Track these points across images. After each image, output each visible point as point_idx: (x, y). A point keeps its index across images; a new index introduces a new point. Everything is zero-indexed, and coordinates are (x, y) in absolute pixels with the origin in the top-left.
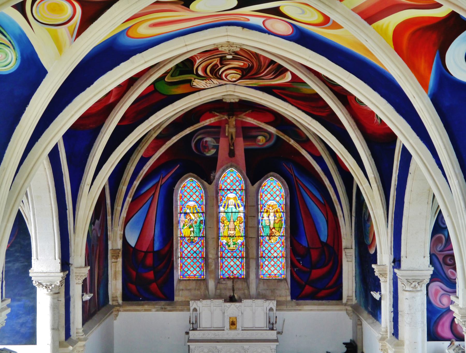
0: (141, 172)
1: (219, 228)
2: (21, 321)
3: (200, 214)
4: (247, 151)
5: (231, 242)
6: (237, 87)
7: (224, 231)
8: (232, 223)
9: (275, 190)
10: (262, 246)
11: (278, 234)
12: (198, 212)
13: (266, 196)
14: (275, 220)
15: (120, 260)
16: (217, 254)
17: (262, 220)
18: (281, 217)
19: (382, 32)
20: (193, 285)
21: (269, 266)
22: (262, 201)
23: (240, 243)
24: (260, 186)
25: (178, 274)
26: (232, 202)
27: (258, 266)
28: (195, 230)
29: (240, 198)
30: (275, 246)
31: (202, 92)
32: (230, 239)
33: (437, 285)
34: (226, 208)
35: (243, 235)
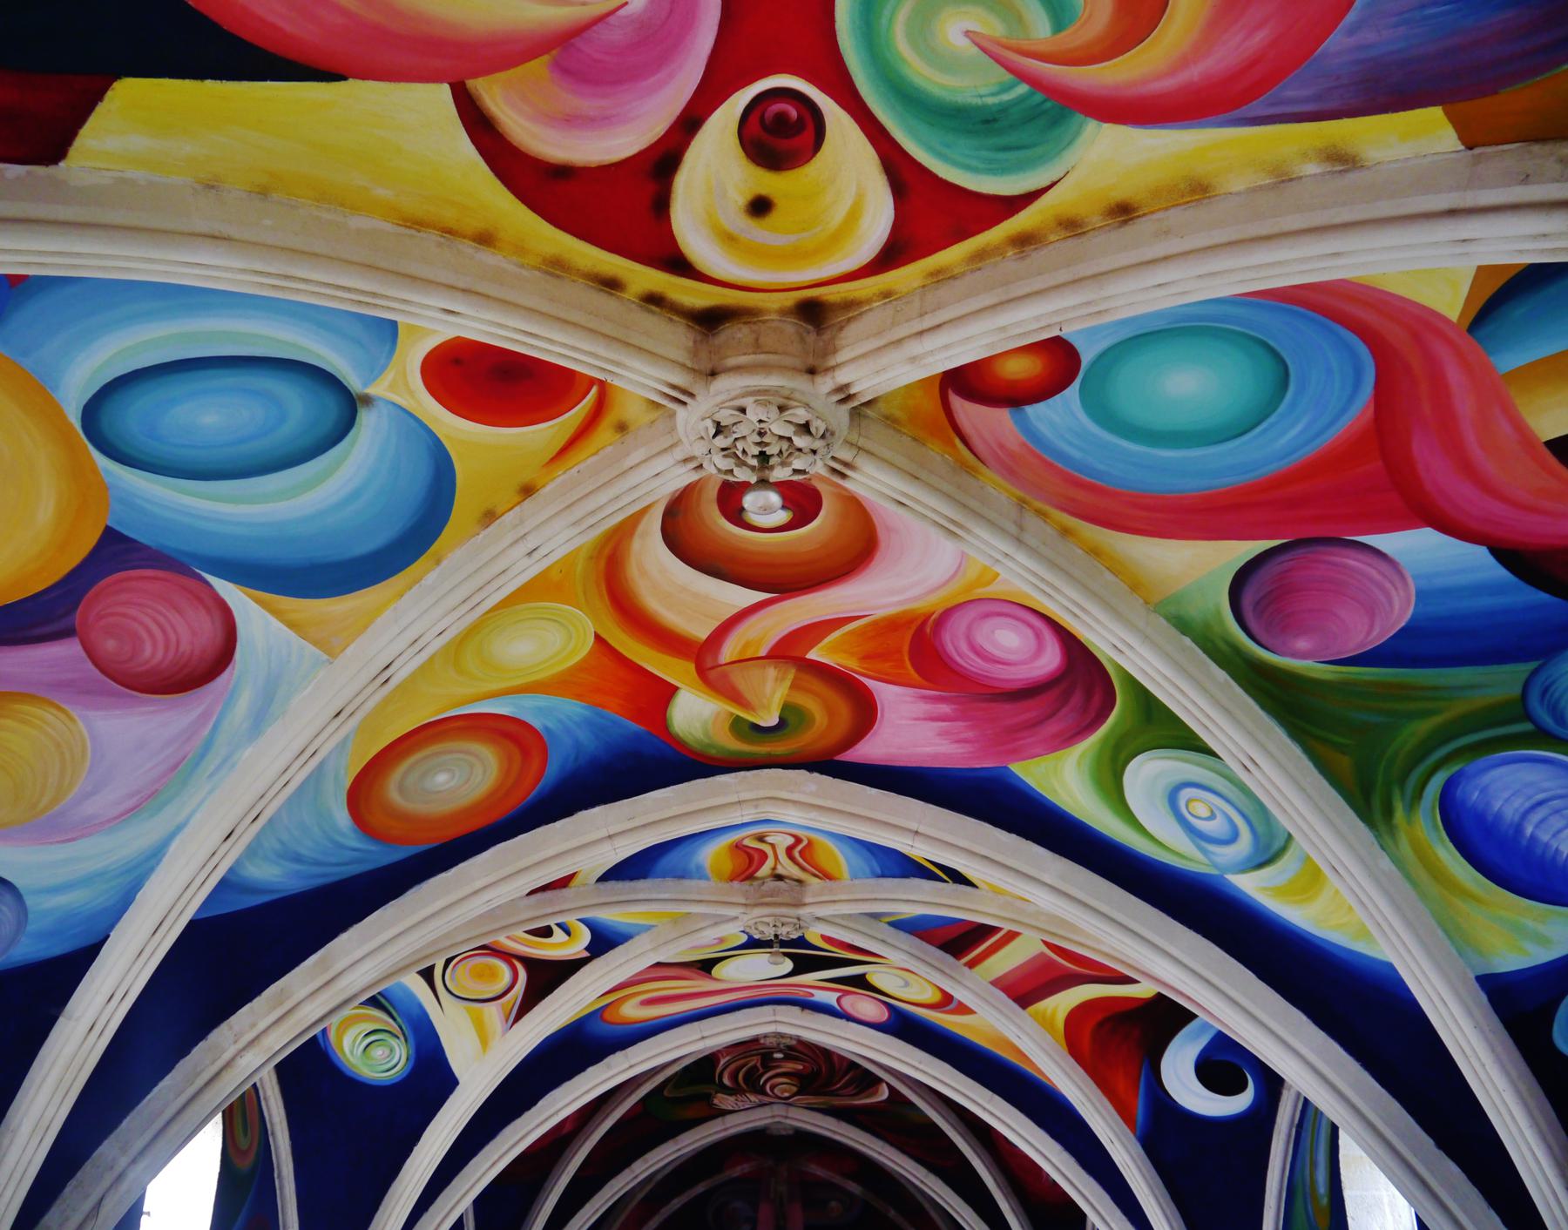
19: (1046, 1023)
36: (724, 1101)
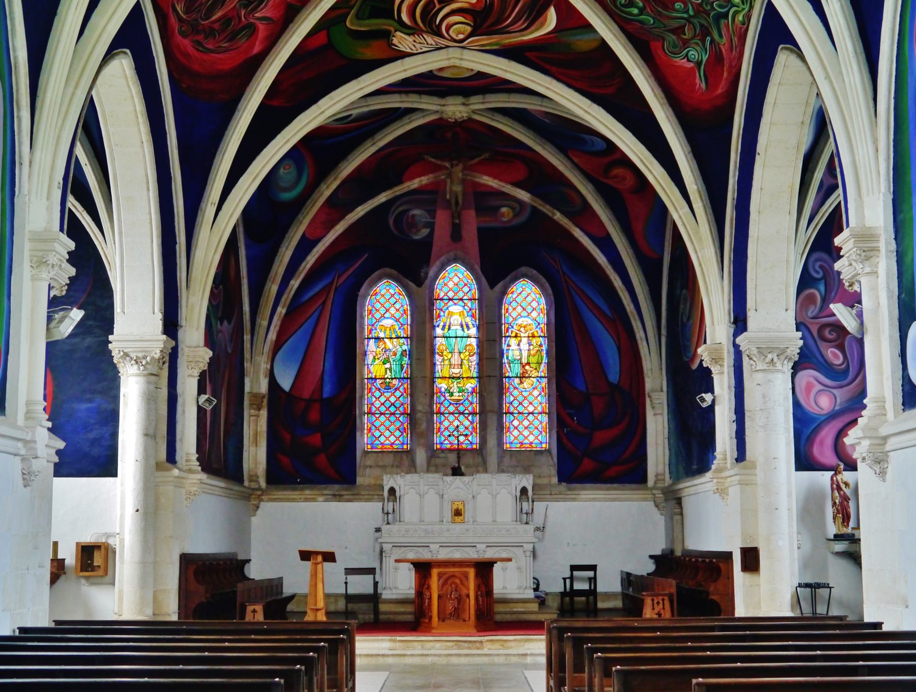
0: (303, 265)
1: (435, 364)
2: (91, 436)
3: (402, 341)
4: (483, 233)
5: (455, 389)
6: (466, 51)
7: (442, 368)
8: (457, 355)
9: (529, 299)
10: (508, 394)
11: (534, 374)
12: (398, 337)
13: (514, 309)
14: (529, 350)
15: (264, 413)
16: (431, 405)
17: (508, 350)
18: (541, 346)
20: (389, 460)
21: (521, 428)
22: (507, 318)
23: (470, 390)
24: (504, 293)
25: (364, 441)
26: (456, 320)
27: (501, 428)
28: (394, 367)
29: (470, 314)
30: (531, 394)
31: (407, 59)
32: (453, 383)
33: (807, 376)
34: (446, 330)
35: (475, 375)
36: (403, 42)
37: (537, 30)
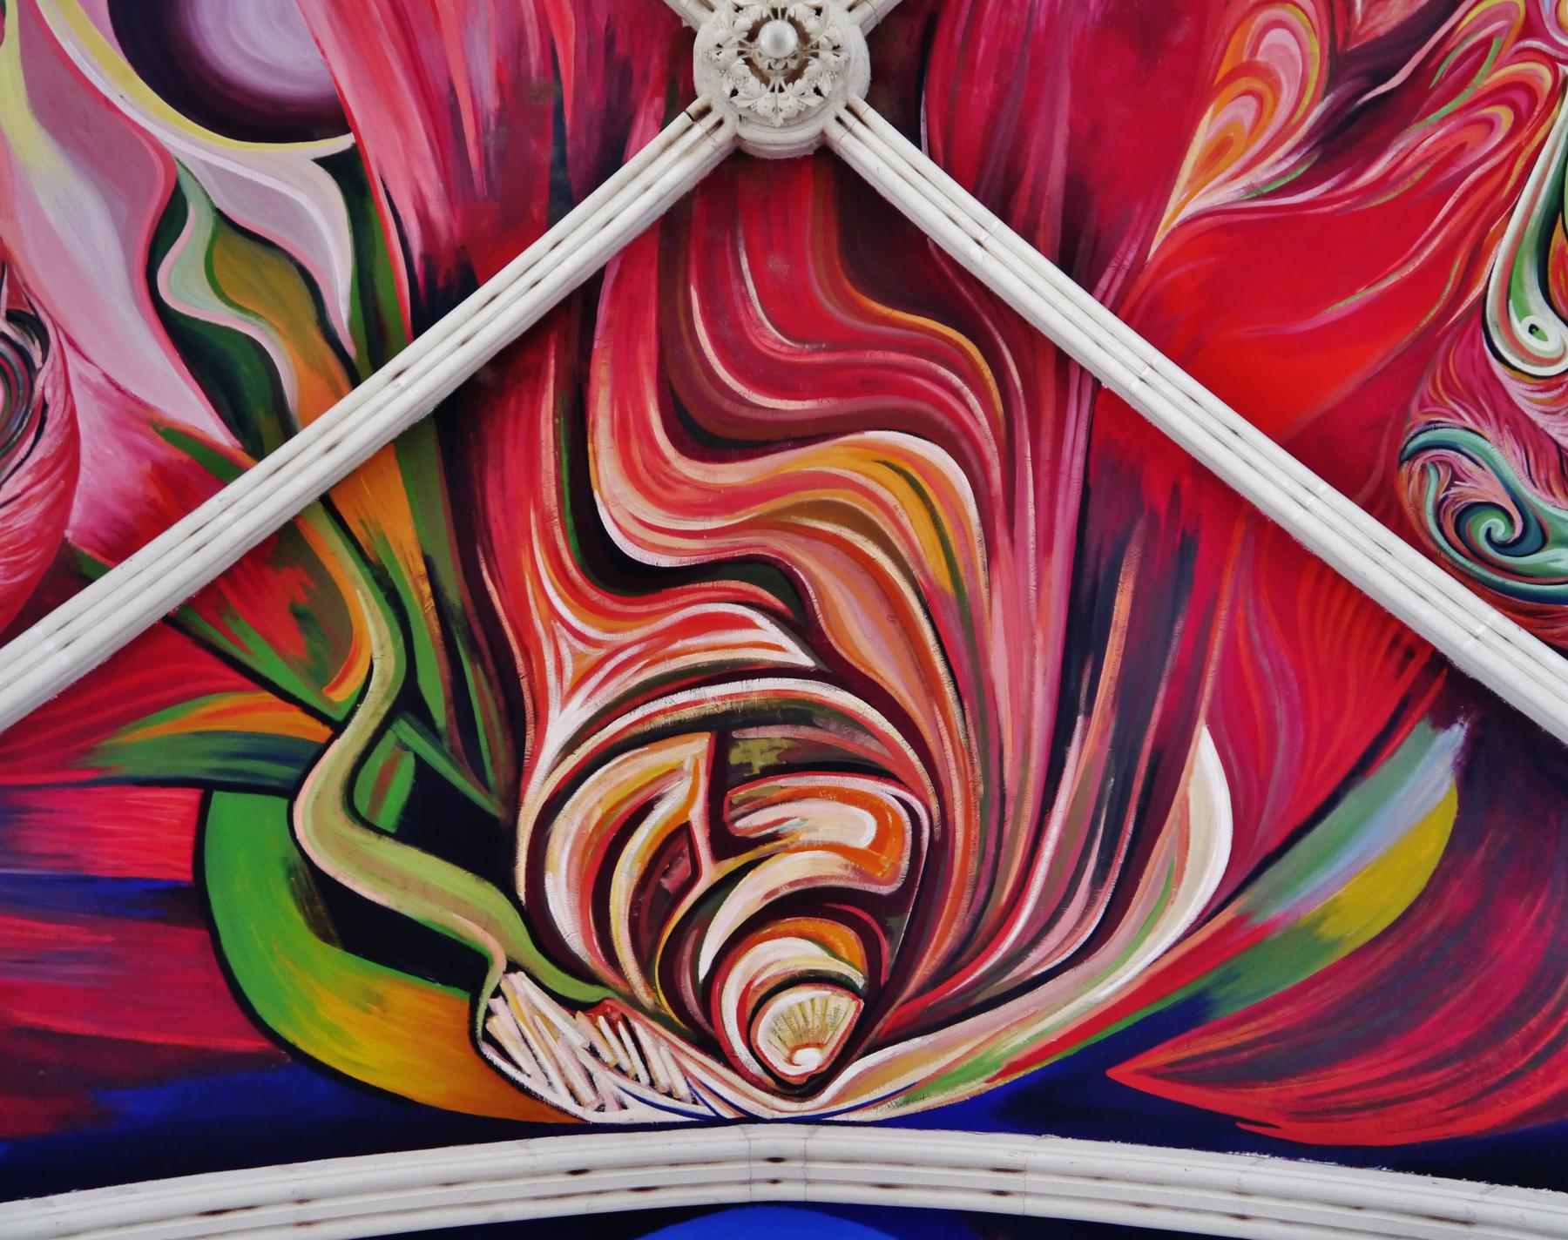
37: (1149, 924)
